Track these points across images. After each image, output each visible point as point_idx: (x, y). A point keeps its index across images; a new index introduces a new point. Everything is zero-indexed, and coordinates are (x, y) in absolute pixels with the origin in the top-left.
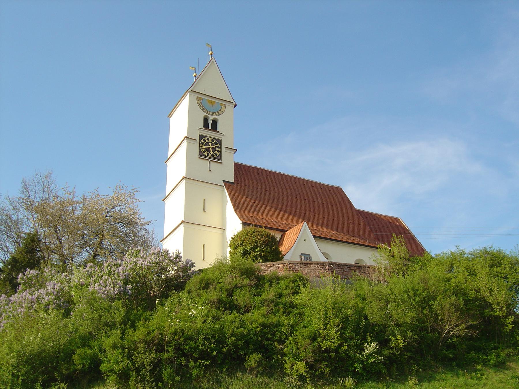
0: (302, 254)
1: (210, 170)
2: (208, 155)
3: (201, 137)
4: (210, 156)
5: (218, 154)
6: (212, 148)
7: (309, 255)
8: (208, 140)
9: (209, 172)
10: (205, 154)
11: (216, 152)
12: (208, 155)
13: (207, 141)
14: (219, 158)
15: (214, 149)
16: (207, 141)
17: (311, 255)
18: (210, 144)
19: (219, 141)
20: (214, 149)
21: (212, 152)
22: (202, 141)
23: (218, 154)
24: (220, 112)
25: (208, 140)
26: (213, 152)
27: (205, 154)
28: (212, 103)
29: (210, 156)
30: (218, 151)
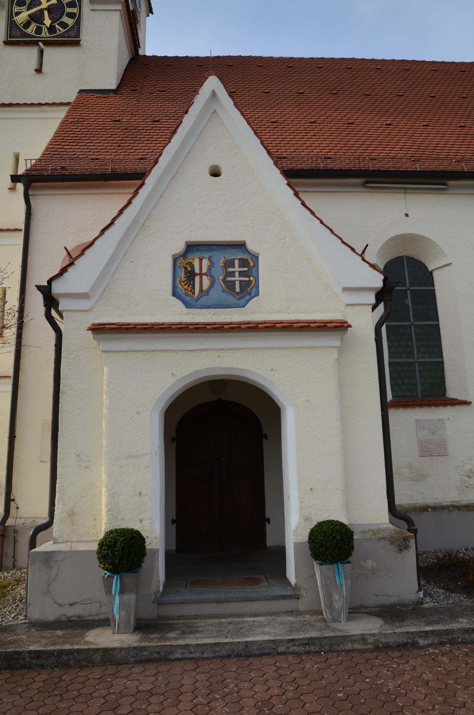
0: (192, 247)
2: (39, 30)
4: (45, 33)
5: (70, 22)
7: (241, 246)
9: (38, 76)
11: (65, 19)
12: (39, 30)
14: (73, 33)
21: (48, 22)
23: (70, 22)
26: (53, 20)
29: (45, 33)
30: (71, 15)
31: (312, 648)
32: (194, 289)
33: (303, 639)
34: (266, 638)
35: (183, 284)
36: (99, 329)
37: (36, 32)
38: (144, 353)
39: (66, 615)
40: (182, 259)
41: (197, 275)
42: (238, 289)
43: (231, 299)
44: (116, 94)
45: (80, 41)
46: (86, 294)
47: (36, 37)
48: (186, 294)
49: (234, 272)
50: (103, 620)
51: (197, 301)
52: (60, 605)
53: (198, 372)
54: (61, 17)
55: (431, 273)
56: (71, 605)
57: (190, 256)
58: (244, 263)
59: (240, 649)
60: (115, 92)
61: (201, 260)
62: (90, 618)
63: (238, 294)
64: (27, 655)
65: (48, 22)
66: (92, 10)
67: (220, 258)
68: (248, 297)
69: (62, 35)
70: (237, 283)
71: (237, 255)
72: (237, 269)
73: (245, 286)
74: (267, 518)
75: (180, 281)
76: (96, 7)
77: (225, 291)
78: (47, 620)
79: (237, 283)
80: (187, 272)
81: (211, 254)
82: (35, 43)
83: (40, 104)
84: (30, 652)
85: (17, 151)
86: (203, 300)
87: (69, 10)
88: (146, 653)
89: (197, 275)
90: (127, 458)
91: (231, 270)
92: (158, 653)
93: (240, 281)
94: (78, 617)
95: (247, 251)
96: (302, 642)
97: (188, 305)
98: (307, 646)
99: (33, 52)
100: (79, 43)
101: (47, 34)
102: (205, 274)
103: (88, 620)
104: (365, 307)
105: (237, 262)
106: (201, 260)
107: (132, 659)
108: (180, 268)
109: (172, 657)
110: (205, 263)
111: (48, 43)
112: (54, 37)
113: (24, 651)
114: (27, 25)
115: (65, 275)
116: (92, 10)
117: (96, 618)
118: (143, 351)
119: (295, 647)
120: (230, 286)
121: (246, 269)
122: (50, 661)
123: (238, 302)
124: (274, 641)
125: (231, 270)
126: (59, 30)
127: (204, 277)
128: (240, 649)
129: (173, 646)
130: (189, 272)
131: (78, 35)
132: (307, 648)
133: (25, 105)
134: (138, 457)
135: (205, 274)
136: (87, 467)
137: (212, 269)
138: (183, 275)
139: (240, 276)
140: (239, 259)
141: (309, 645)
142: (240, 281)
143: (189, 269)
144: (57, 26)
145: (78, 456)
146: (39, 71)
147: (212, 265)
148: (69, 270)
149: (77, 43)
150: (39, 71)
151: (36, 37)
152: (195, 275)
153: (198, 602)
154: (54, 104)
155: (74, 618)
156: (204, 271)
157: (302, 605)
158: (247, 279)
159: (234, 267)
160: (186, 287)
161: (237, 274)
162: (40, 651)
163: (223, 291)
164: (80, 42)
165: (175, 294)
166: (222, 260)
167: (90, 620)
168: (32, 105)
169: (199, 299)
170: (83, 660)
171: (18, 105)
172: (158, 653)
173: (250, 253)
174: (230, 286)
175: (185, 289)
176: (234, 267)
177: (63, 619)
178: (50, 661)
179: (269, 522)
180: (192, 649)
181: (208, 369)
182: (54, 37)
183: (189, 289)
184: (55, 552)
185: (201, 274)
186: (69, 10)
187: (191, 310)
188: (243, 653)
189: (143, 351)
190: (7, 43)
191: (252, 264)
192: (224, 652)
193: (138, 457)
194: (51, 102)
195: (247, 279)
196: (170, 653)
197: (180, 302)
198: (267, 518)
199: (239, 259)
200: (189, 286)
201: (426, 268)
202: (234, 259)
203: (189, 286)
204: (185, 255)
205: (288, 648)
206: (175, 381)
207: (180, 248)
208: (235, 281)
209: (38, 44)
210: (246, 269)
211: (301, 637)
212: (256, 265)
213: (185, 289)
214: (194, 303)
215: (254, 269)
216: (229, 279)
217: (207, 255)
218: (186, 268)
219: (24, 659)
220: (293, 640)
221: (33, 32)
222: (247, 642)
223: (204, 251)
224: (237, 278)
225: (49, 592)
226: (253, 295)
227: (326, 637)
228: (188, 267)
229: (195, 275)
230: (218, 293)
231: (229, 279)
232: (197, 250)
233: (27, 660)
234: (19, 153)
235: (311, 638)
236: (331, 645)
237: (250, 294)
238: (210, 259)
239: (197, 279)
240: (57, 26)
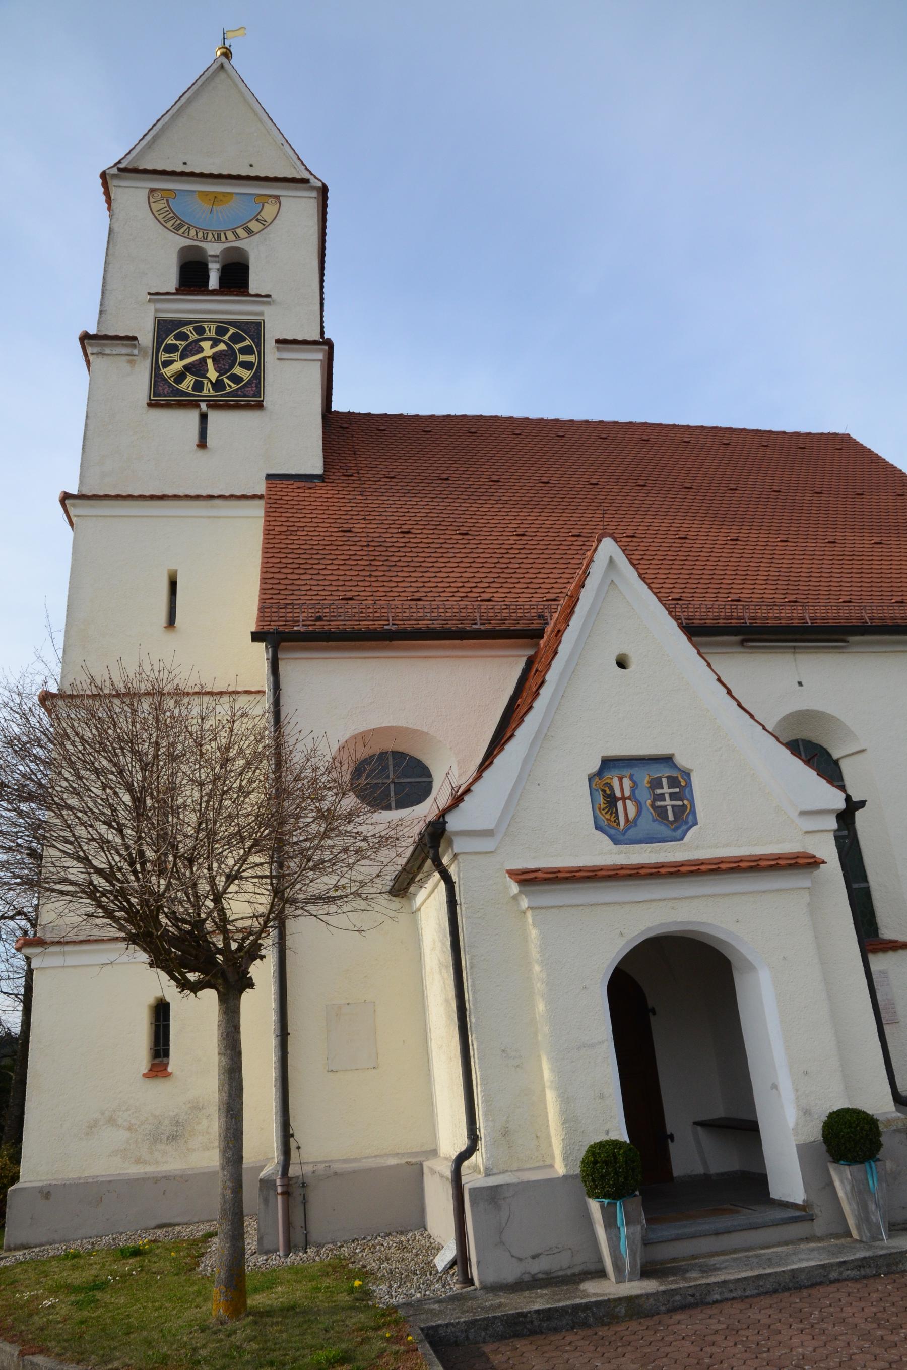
0: (608, 763)
1: (202, 443)
2: (198, 386)
3: (164, 327)
4: (208, 390)
5: (246, 374)
6: (215, 358)
7: (667, 760)
8: (200, 330)
9: (201, 453)
10: (183, 386)
11: (238, 370)
12: (198, 386)
13: (194, 336)
14: (250, 390)
15: (224, 361)
16: (194, 336)
17: (682, 760)
18: (206, 345)
19: (255, 330)
20: (224, 361)
21: (213, 375)
22: (171, 340)
23: (246, 374)
24: (254, 226)
25: (200, 330)
26: (221, 371)
27: (183, 386)
28: (216, 198)
29: (208, 390)
30: (247, 366)
31: (868, 1271)
32: (618, 818)
33: (856, 1260)
34: (813, 1263)
35: (603, 812)
36: (529, 879)
37: (194, 389)
38: (581, 908)
39: (529, 1273)
40: (597, 779)
41: (619, 799)
42: (671, 817)
43: (661, 829)
44: (324, 482)
45: (263, 401)
46: (492, 830)
47: (194, 396)
48: (609, 825)
49: (663, 794)
50: (580, 1274)
51: (624, 834)
52: (520, 1259)
53: (650, 929)
54: (232, 367)
55: (836, 763)
56: (534, 1257)
57: (607, 775)
58: (673, 782)
59: (787, 1281)
61: (621, 779)
62: (561, 1273)
63: (672, 823)
64: (535, 1316)
65: (213, 375)
66: (279, 359)
67: (644, 777)
68: (684, 827)
69: (233, 394)
70: (669, 809)
71: (664, 772)
72: (666, 790)
73: (679, 811)
74: (668, 1133)
75: (600, 809)
76: (285, 355)
77: (657, 820)
78: (505, 1282)
79: (669, 809)
80: (606, 796)
81: (633, 771)
82: (195, 405)
83: (211, 497)
84: (538, 1312)
85: (174, 567)
86: (631, 833)
87: (242, 358)
88: (678, 1298)
89: (619, 799)
90: (579, 1048)
91: (659, 791)
92: (693, 1296)
93: (673, 806)
94: (546, 1273)
95: (675, 766)
96: (856, 1263)
97: (616, 842)
98: (862, 1269)
99: (191, 418)
100: (262, 406)
101: (211, 391)
102: (629, 798)
103: (558, 1277)
104: (825, 833)
105: (664, 781)
106: (621, 779)
107: (663, 1308)
108: (597, 790)
109: (709, 1299)
110: (627, 783)
111: (215, 405)
112: (222, 396)
113: (530, 1312)
114: (180, 377)
115: (461, 805)
116: (279, 359)
117: (569, 1272)
118: (582, 905)
119: (849, 1272)
120: (661, 813)
121: (677, 790)
122: (564, 1322)
123: (674, 834)
124: (823, 1266)
125: (659, 791)
126: (230, 386)
127: (628, 802)
128: (787, 1281)
129: (709, 1284)
130: (608, 796)
131: (258, 393)
132: (863, 1272)
133: (187, 497)
134: (592, 1046)
135: (629, 798)
136: (517, 1066)
137: (637, 792)
138: (602, 801)
139: (671, 800)
140: (668, 777)
141: (864, 1267)
142: (673, 806)
143: (608, 792)
144: (226, 380)
145: (503, 1051)
146: (202, 443)
147: (635, 786)
148: (466, 798)
151: (194, 396)
152: (618, 799)
153: (693, 1236)
154: (232, 497)
155: (541, 1276)
156: (627, 794)
157: (819, 1227)
158: (680, 803)
159: (662, 788)
160: (608, 816)
161: (667, 797)
162: (550, 1309)
163: (654, 821)
164: (264, 404)
165: (598, 827)
166: (647, 779)
167: (562, 1276)
168: (198, 497)
169: (626, 832)
170: (604, 1316)
171: (176, 497)
172: (693, 1296)
173: (679, 769)
174: (661, 813)
175: (608, 819)
176: (662, 788)
177: (527, 1278)
178: (564, 1322)
179: (672, 1140)
180: (731, 1286)
181: (661, 925)
182: (222, 396)
183: (613, 819)
184: (501, 1185)
185: (624, 799)
186: (242, 358)
187: (623, 847)
188: (791, 1285)
189: (582, 905)
190: (152, 405)
191: (683, 784)
192: (769, 1287)
193: (592, 1046)
194: (227, 495)
195: (680, 803)
196: (706, 1295)
197: (606, 838)
198: (668, 1133)
199: (668, 777)
200: (611, 814)
201: (829, 755)
202: (661, 777)
203: (611, 814)
204: (600, 773)
205: (841, 1273)
206: (624, 942)
207: (595, 766)
208: (666, 806)
209: (199, 406)
210: (677, 790)
211: (852, 1257)
212: (689, 784)
213: (608, 819)
214: (621, 837)
215: (687, 790)
216: (659, 803)
217: (627, 772)
218: (604, 791)
219: (532, 1322)
220: (844, 1262)
221: (190, 388)
222: (793, 1270)
223: (624, 767)
224: (668, 802)
225: (502, 1243)
226: (691, 823)
227: (881, 1256)
228: (607, 789)
229: (618, 799)
230: (648, 823)
231: (659, 803)
232: (615, 767)
233: (536, 1323)
234: (176, 571)
235: (865, 1258)
236: (888, 1265)
237: (686, 822)
238: (631, 778)
239: (620, 804)
240: (226, 380)
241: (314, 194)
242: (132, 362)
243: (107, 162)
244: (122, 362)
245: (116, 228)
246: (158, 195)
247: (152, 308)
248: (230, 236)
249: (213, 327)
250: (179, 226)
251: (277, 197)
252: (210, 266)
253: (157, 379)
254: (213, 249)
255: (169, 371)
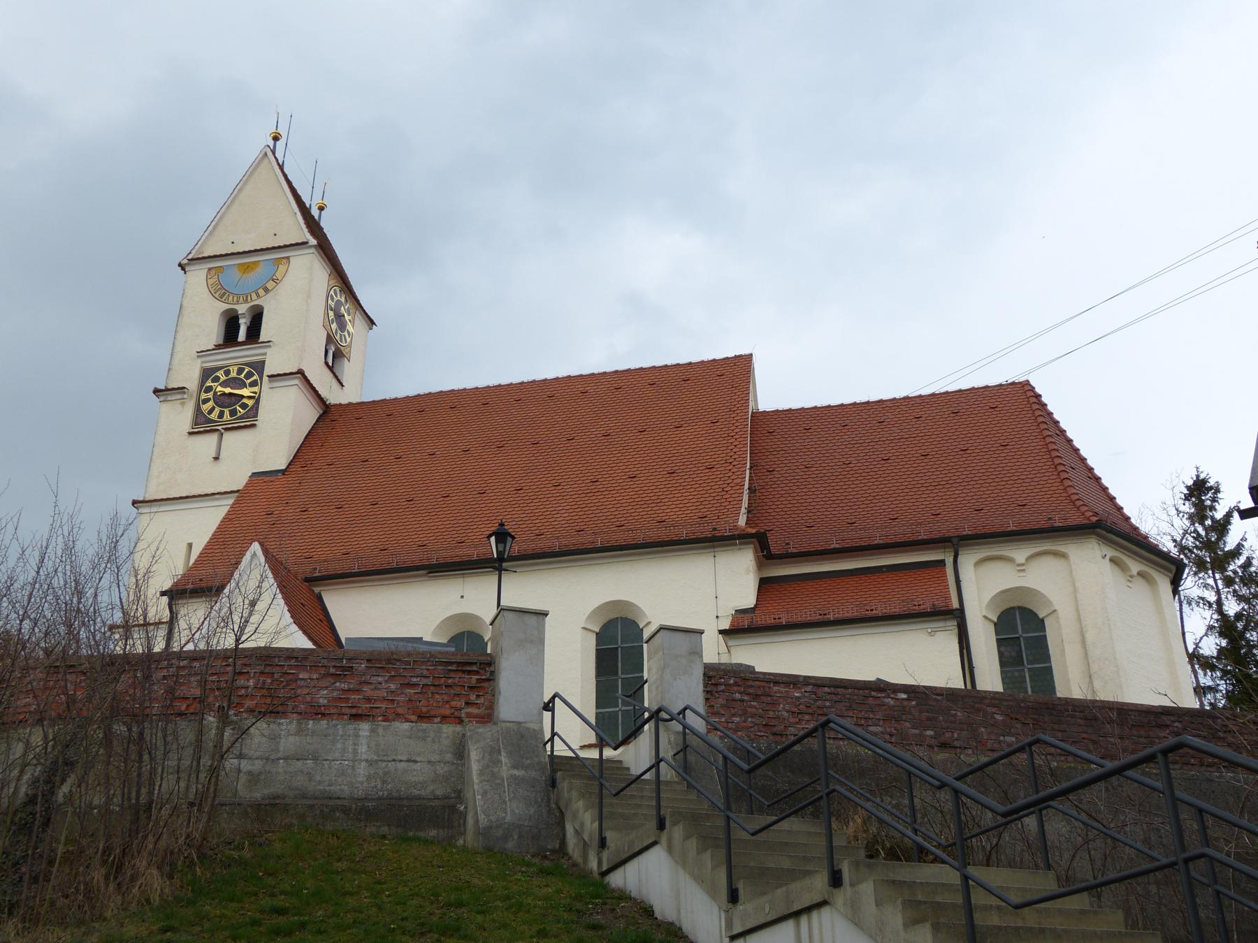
3: (207, 374)
22: (209, 383)
24: (270, 285)
60: (283, 472)
76: (275, 384)
114: (211, 412)
131: (256, 416)
149: (254, 426)
150: (216, 458)
241: (313, 250)
242: (183, 404)
243: (181, 257)
244: (177, 405)
245: (185, 304)
246: (213, 272)
247: (199, 361)
248: (254, 296)
249: (236, 368)
250: (221, 298)
251: (288, 258)
252: (242, 321)
253: (198, 410)
254: (242, 309)
255: (205, 408)
